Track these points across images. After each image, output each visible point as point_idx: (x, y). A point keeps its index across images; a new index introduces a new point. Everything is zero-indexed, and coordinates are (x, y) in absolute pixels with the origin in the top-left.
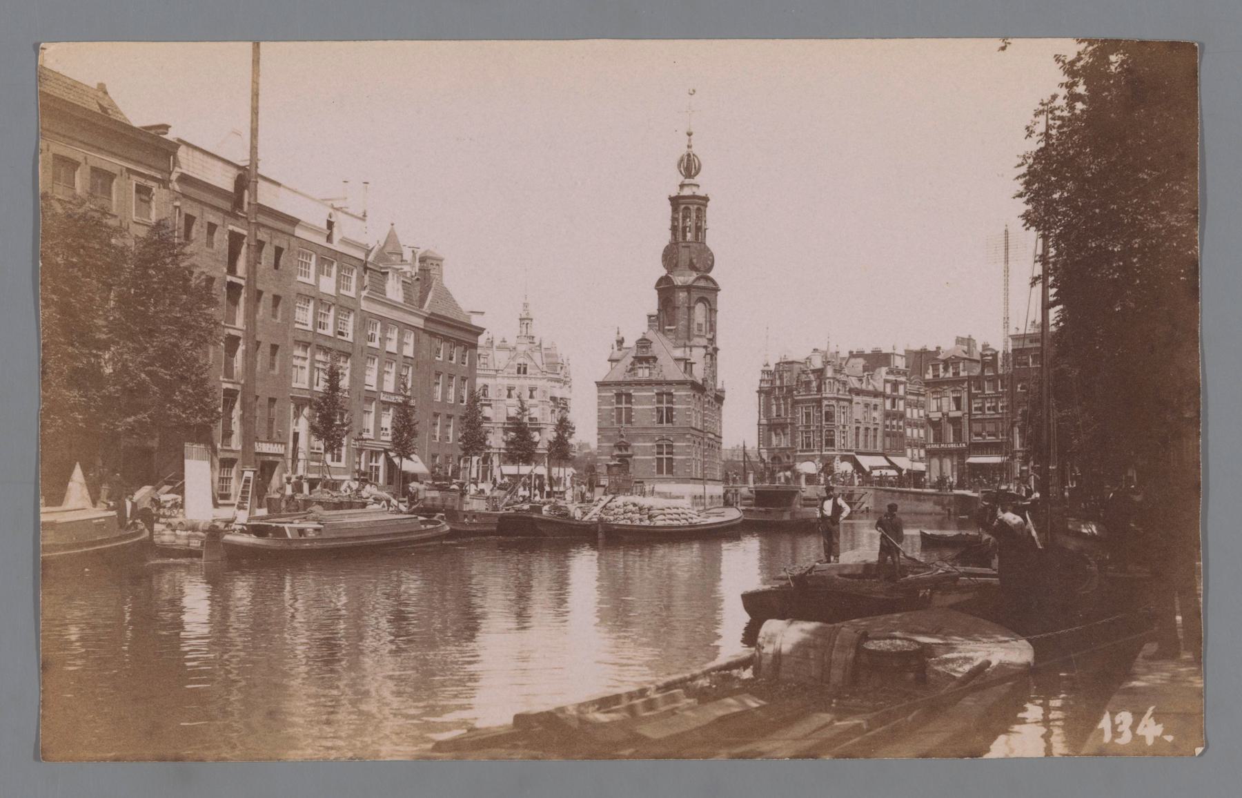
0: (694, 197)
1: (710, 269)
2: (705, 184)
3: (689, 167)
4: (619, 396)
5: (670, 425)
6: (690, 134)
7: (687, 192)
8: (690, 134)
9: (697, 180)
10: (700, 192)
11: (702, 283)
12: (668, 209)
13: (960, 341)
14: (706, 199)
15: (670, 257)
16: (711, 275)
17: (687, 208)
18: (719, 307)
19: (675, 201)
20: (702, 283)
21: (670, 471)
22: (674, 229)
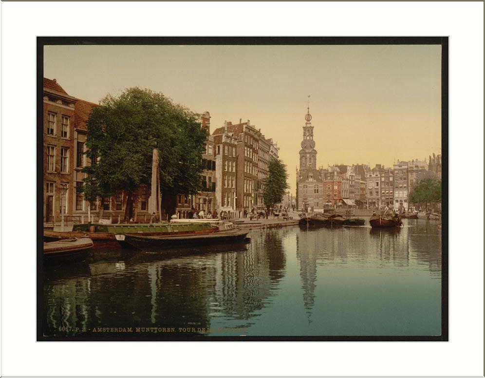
0: (311, 127)
1: (314, 147)
2: (313, 123)
3: (308, 117)
4: (304, 186)
5: (318, 194)
6: (308, 108)
7: (308, 125)
8: (308, 108)
9: (310, 122)
10: (312, 126)
11: (313, 152)
12: (302, 131)
13: (377, 165)
16: (315, 149)
18: (317, 158)
20: (313, 152)
21: (317, 206)
22: (304, 135)
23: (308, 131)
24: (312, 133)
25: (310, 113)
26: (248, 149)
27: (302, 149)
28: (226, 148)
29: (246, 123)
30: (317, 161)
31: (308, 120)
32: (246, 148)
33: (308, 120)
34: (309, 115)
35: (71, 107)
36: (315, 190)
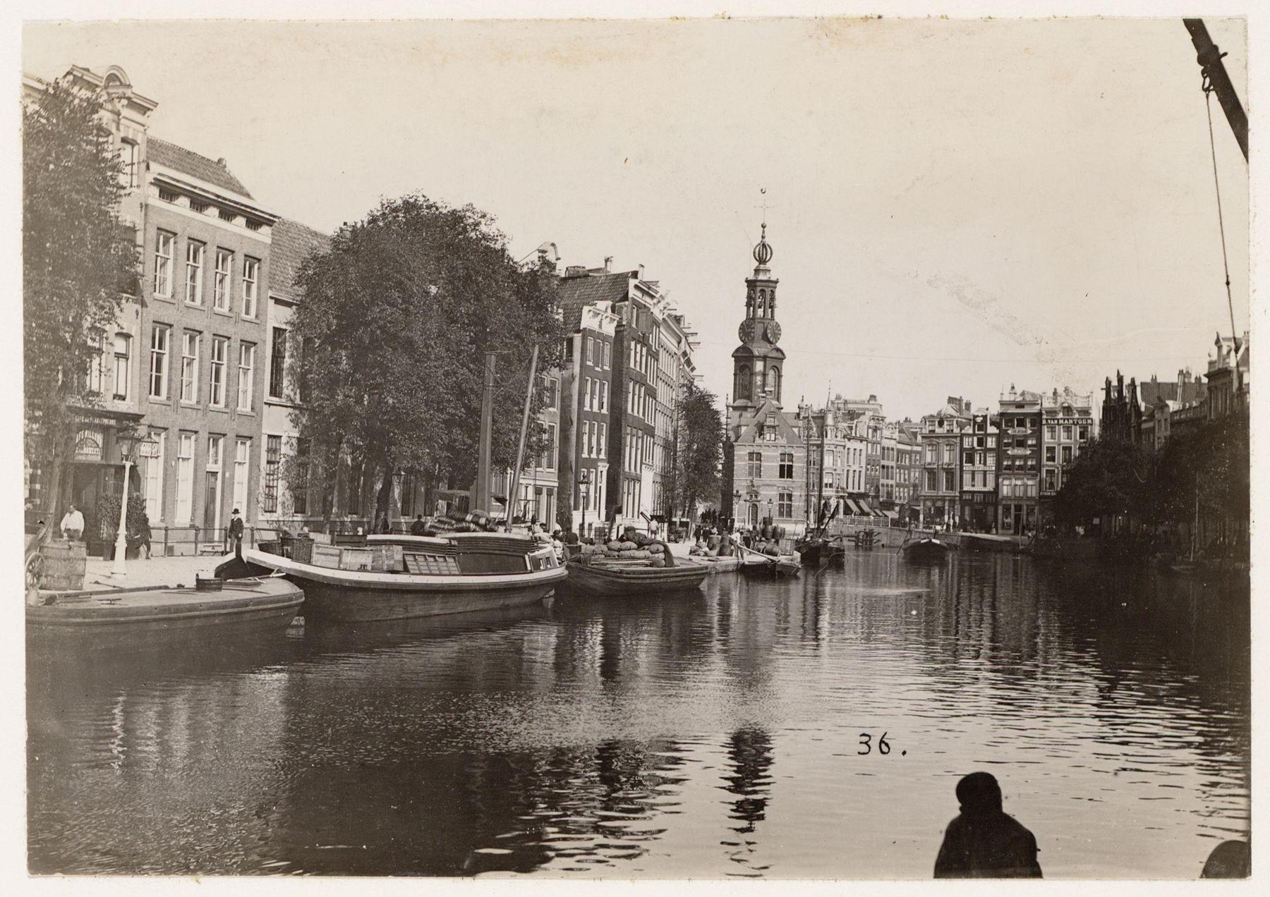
0: (769, 281)
2: (775, 269)
3: (762, 255)
7: (762, 277)
8: (763, 227)
9: (768, 265)
10: (773, 279)
12: (744, 290)
14: (776, 282)
15: (746, 330)
16: (779, 345)
17: (763, 291)
18: (783, 373)
19: (751, 284)
20: (774, 354)
22: (748, 305)
23: (760, 292)
24: (773, 299)
25: (767, 241)
26: (639, 346)
27: (741, 343)
28: (590, 343)
29: (635, 274)
30: (783, 379)
31: (762, 261)
32: (633, 344)
33: (762, 261)
34: (764, 245)
35: (264, 234)
36: (782, 467)
